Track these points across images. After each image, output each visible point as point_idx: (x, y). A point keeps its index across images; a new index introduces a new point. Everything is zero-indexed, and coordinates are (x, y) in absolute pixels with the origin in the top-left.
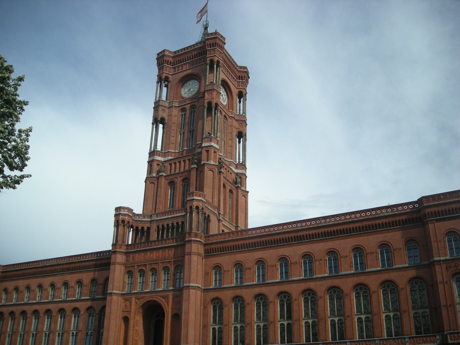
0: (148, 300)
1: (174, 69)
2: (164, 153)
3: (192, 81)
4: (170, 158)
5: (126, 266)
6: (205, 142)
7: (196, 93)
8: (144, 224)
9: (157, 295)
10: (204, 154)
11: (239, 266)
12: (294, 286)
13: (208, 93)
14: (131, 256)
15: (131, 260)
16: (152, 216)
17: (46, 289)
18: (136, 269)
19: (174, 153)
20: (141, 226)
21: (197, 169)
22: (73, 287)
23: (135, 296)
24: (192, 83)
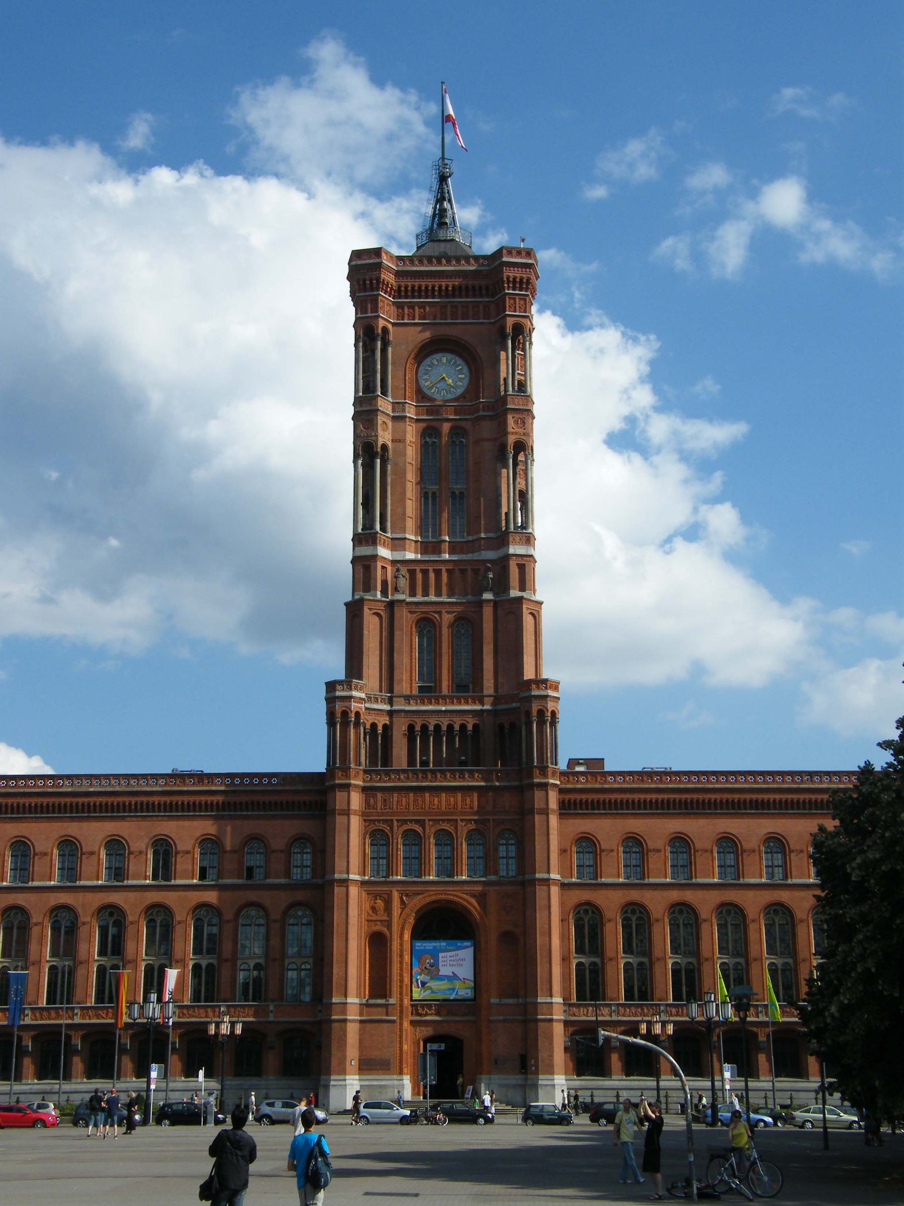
0: (434, 898)
1: (398, 308)
2: (392, 539)
3: (450, 356)
4: (410, 556)
5: (365, 818)
6: (515, 543)
7: (462, 397)
8: (377, 718)
9: (459, 888)
10: (514, 572)
11: (634, 843)
12: (750, 894)
13: (517, 416)
14: (379, 795)
15: (379, 804)
16: (395, 699)
17: (92, 853)
18: (395, 828)
19: (413, 543)
20: (371, 722)
21: (496, 604)
22: (188, 852)
23: (399, 889)
24: (449, 361)
